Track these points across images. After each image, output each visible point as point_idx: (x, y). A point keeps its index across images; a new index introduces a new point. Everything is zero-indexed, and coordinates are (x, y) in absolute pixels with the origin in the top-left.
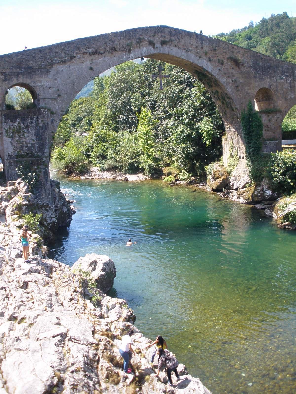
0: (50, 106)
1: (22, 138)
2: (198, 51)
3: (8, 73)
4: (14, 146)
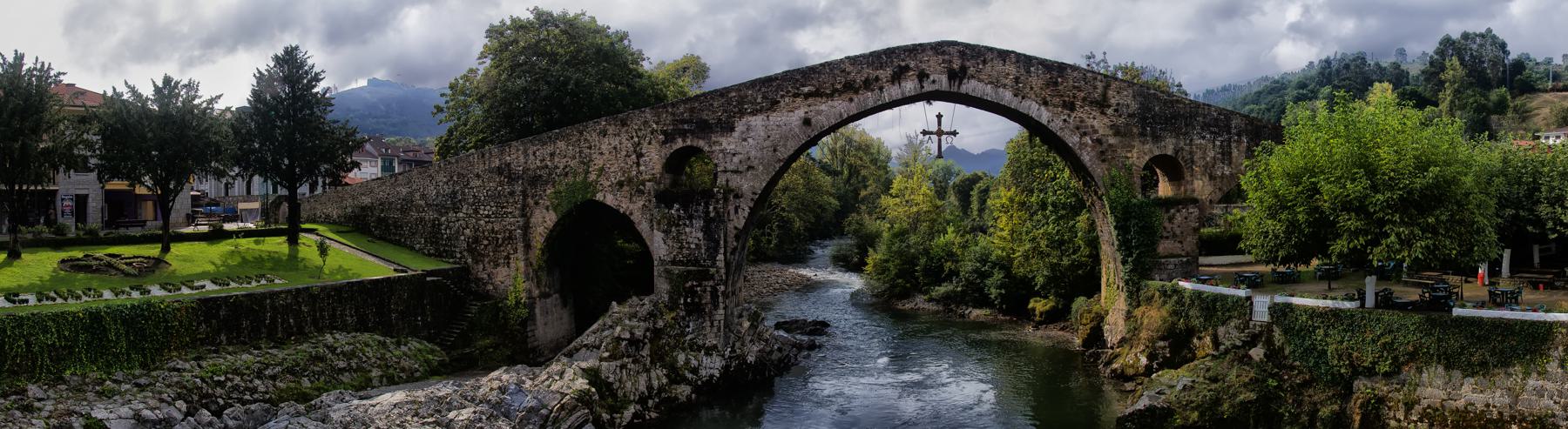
0: (733, 185)
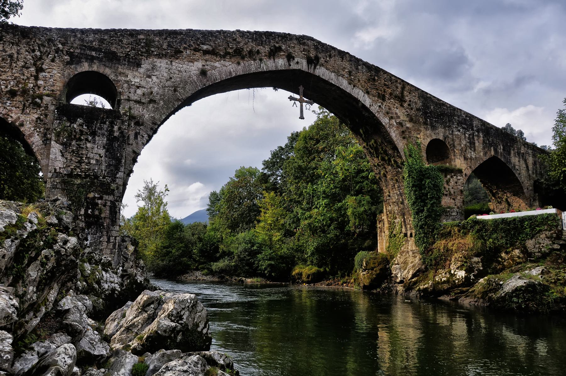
1: (83, 148)
2: (352, 77)
3: (77, 54)
4: (66, 159)
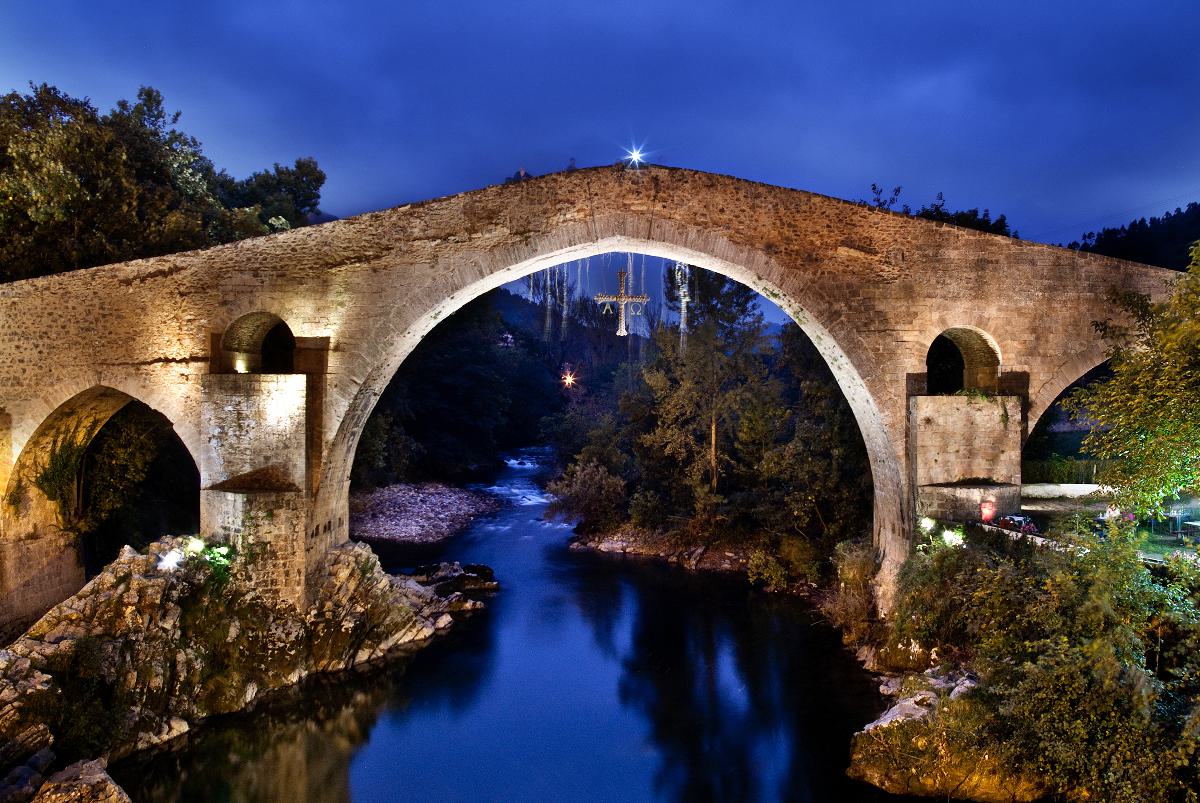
3: (230, 288)
